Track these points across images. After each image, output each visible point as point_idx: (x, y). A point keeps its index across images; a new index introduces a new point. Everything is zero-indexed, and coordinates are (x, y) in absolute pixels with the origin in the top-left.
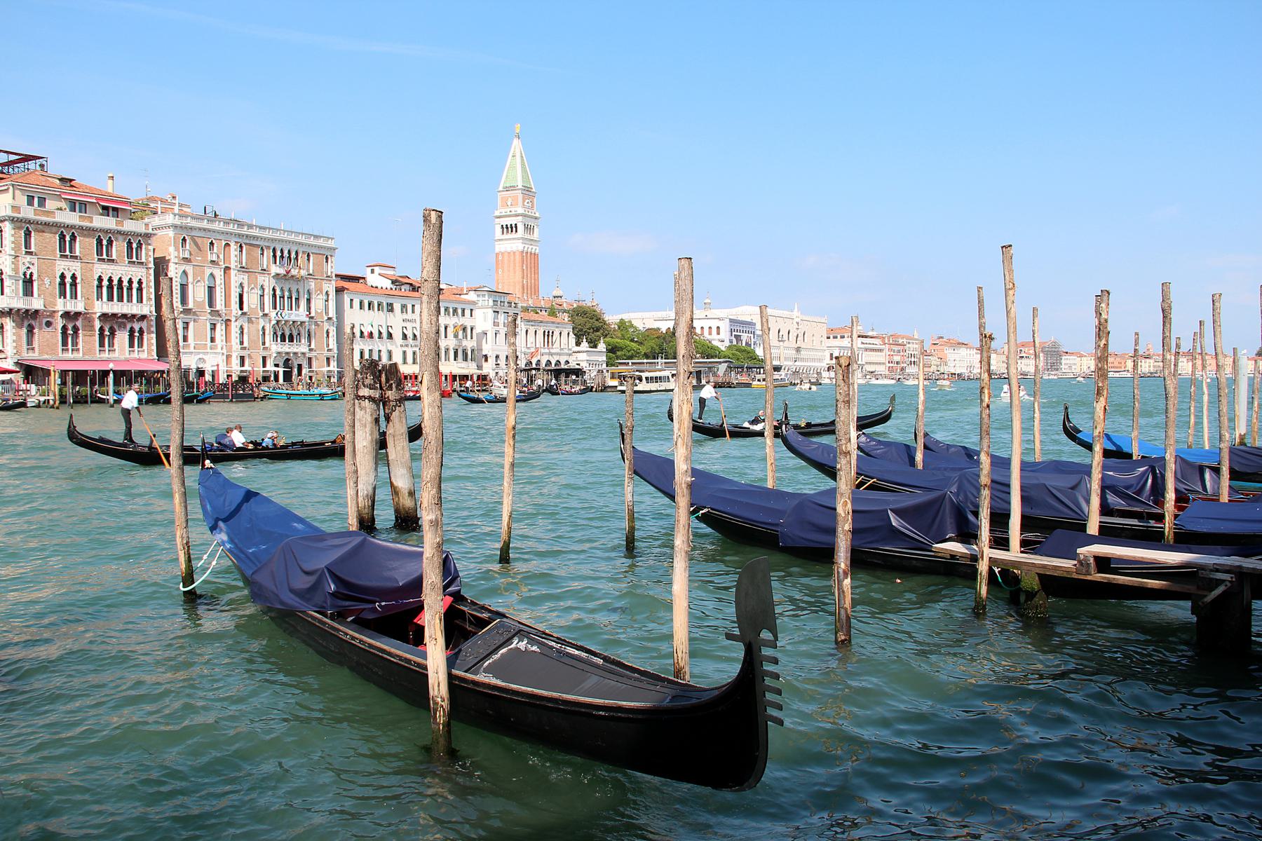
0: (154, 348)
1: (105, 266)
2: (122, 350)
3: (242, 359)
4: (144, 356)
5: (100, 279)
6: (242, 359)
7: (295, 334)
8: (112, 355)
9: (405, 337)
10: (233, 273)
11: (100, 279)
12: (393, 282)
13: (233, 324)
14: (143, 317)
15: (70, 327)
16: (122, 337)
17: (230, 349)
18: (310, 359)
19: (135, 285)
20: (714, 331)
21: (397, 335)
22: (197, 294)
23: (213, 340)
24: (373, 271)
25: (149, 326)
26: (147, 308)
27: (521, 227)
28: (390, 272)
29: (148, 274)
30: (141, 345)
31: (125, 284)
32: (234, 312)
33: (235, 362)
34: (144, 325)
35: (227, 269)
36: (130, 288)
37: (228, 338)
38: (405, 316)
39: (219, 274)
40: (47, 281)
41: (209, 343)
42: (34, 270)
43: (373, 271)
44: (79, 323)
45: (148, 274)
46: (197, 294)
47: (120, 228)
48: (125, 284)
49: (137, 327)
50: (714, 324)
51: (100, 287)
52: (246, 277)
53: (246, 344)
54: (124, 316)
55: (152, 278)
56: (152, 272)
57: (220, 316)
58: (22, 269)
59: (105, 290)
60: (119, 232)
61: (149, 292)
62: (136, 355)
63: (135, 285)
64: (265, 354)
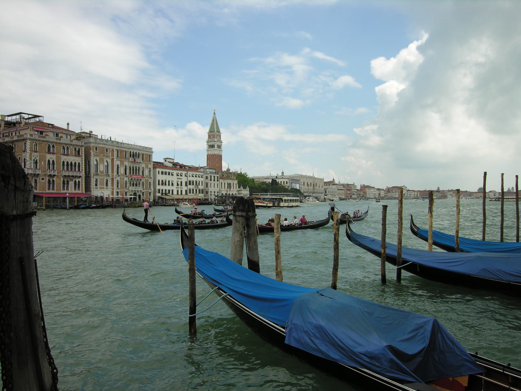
0: (84, 188)
1: (65, 157)
2: (71, 189)
3: (118, 192)
4: (80, 192)
5: (64, 162)
6: (118, 192)
7: (138, 183)
8: (67, 192)
9: (178, 185)
10: (115, 160)
11: (64, 162)
12: (173, 165)
13: (115, 179)
14: (80, 177)
15: (51, 180)
16: (71, 184)
17: (113, 189)
18: (143, 193)
19: (77, 165)
20: (285, 183)
22: (101, 168)
23: (107, 185)
24: (166, 161)
25: (82, 180)
26: (83, 174)
27: (216, 146)
28: (172, 161)
29: (82, 161)
31: (73, 164)
32: (115, 175)
33: (115, 193)
34: (80, 180)
35: (113, 160)
36: (75, 166)
37: (113, 185)
40: (43, 163)
41: (105, 187)
42: (38, 158)
43: (166, 161)
44: (55, 179)
45: (82, 161)
47: (71, 143)
48: (73, 164)
49: (77, 180)
50: (285, 180)
51: (63, 165)
53: (119, 187)
54: (73, 176)
55: (84, 162)
56: (83, 160)
58: (33, 158)
59: (65, 166)
60: (71, 145)
61: (83, 167)
62: (77, 191)
63: (77, 165)
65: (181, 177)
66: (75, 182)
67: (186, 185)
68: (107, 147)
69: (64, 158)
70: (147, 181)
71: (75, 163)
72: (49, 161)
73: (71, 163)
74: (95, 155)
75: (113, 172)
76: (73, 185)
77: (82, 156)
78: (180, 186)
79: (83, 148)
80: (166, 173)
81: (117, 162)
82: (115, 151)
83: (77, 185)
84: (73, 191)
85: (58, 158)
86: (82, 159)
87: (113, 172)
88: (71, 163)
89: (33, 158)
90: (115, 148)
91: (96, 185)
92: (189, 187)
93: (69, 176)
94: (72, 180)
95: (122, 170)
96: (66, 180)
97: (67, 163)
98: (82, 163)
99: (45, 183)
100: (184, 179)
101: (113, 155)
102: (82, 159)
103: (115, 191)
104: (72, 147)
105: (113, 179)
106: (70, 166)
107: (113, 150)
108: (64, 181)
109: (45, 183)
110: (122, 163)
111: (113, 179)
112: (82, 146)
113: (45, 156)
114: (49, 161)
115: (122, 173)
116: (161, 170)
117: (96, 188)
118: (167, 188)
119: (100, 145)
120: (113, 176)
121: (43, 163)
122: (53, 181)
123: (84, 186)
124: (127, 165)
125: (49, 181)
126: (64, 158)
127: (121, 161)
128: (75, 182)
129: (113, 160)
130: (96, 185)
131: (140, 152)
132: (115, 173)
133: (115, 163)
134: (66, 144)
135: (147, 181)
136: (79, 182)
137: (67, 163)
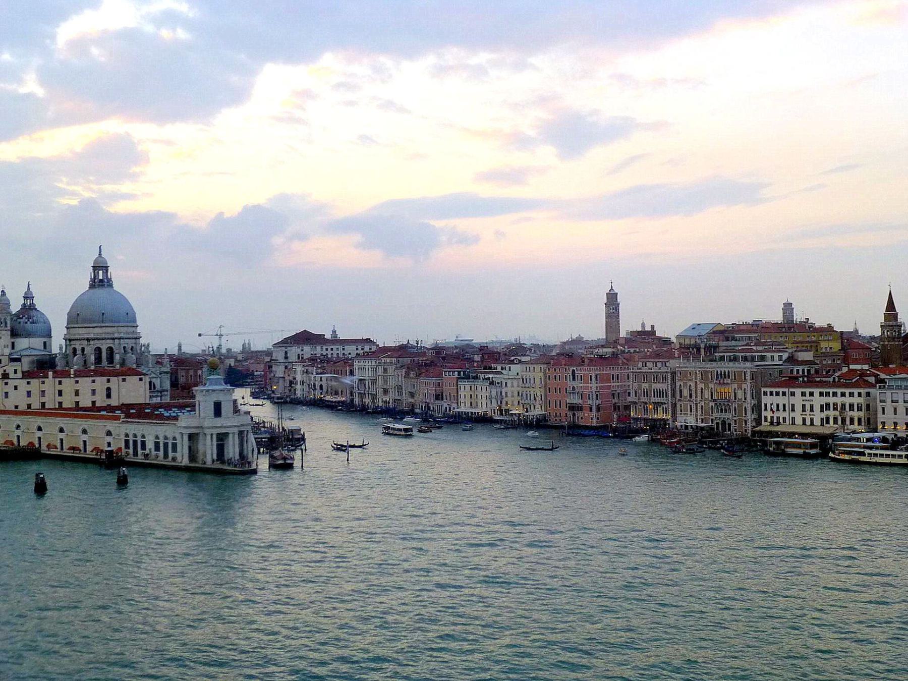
16: (660, 409)
21: (799, 408)
22: (686, 393)
38: (804, 398)
39: (693, 385)
65: (811, 398)
67: (822, 411)
78: (808, 412)
80: (777, 394)
81: (701, 386)
92: (826, 413)
95: (707, 394)
100: (818, 401)
101: (696, 378)
106: (661, 394)
110: (706, 386)
116: (768, 390)
132: (699, 398)
135: (740, 406)
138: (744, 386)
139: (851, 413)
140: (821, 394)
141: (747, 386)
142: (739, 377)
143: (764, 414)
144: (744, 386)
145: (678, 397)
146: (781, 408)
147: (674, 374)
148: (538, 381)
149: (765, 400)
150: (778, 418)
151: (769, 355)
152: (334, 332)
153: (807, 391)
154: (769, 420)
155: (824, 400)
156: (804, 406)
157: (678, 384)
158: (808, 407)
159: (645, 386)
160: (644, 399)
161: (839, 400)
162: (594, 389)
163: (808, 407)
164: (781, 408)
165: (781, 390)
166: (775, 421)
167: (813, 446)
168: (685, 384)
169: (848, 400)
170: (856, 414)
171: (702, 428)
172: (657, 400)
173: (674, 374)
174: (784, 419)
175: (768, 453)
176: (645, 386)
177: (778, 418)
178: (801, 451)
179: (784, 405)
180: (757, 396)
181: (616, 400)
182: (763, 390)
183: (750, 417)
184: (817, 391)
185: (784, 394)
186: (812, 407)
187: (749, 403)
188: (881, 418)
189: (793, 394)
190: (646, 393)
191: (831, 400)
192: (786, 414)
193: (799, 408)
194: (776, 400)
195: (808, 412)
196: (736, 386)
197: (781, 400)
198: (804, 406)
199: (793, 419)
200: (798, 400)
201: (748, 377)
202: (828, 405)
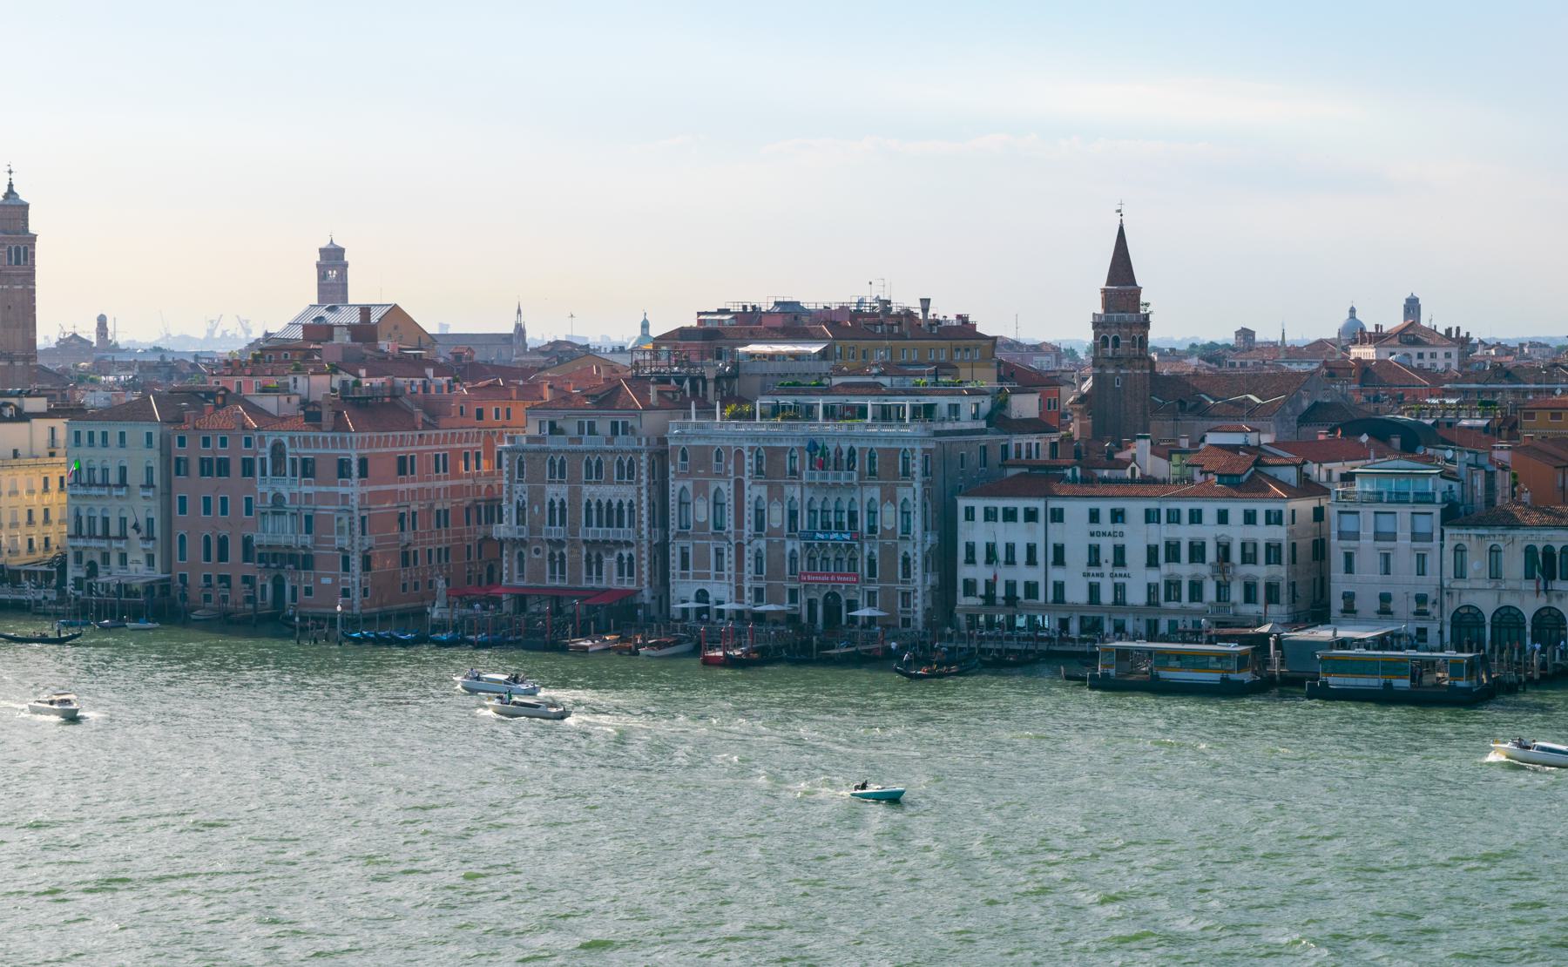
1: (593, 488)
2: (610, 579)
5: (588, 504)
11: (588, 504)
13: (747, 548)
16: (610, 561)
17: (740, 579)
21: (1077, 556)
22: (701, 511)
23: (719, 567)
30: (631, 574)
34: (634, 551)
35: (739, 485)
38: (1095, 527)
39: (727, 488)
40: (536, 509)
41: (712, 571)
44: (565, 550)
45: (639, 494)
46: (701, 511)
48: (615, 506)
49: (625, 553)
52: (764, 489)
57: (727, 539)
58: (515, 498)
64: (794, 586)
65: (1119, 527)
66: (621, 557)
67: (1152, 561)
68: (718, 443)
69: (590, 491)
70: (888, 552)
71: (620, 504)
72: (552, 503)
73: (609, 503)
74: (678, 476)
75: (739, 524)
76: (615, 567)
77: (639, 481)
78: (1107, 568)
79: (644, 457)
80: (1010, 515)
81: (754, 492)
82: (747, 454)
83: (627, 567)
84: (615, 585)
85: (575, 493)
86: (639, 489)
87: (739, 524)
88: (609, 503)
89: (515, 498)
90: (747, 445)
91: (685, 566)
92: (1166, 569)
93: (606, 542)
94: (610, 552)
95: (776, 517)
96: (594, 554)
97: (599, 503)
98: (640, 502)
99: (542, 562)
100: (1138, 537)
101: (739, 469)
102: (639, 489)
103: (747, 585)
104: (609, 458)
105: (740, 548)
106: (612, 514)
107: (739, 453)
108: (588, 556)
109: (542, 562)
110: (775, 493)
111: (740, 548)
112: (638, 452)
113: (542, 490)
114: (552, 503)
115: (776, 525)
116: (979, 504)
117: (682, 576)
118: (1022, 574)
119: (694, 443)
120: (739, 536)
121: (536, 509)
122: (562, 555)
123: (645, 569)
124: (797, 495)
125: (552, 556)
126: (590, 491)
127: (770, 486)
128: (621, 557)
129: (739, 485)
130: (685, 566)
131: (856, 446)
132: (749, 528)
133: (747, 492)
134: (594, 452)
135: (888, 552)
136: (631, 558)
137: (599, 503)
138: (903, 493)
139: (1249, 569)
140: (1151, 517)
141: (912, 492)
142: (885, 467)
143: (964, 572)
144: (903, 493)
145: (674, 526)
146: (1021, 555)
147: (660, 456)
148: (136, 477)
149: (976, 533)
150: (1011, 586)
151: (943, 402)
152: (102, 322)
153: (1105, 507)
154: (981, 590)
155: (1161, 533)
156: (1094, 551)
157: (675, 487)
158: (1107, 554)
159: (556, 492)
160: (557, 532)
161: (1209, 532)
162: (355, 502)
163: (1107, 554)
164: (1021, 555)
165: (1021, 504)
166: (1000, 591)
167: (1242, 662)
168: (701, 489)
169: (1236, 532)
170: (1261, 572)
171: (759, 618)
172: (602, 533)
173: (660, 456)
174: (1031, 589)
175: (1104, 685)
176: (556, 492)
177: (1011, 586)
178: (1213, 677)
179: (1031, 549)
180: (945, 524)
181: (408, 536)
182: (963, 503)
183: (921, 582)
184: (1135, 509)
185: (1031, 516)
186: (1119, 552)
187: (918, 545)
188: (1339, 583)
189: (1057, 516)
190: (558, 513)
191: (1185, 533)
192: (1034, 574)
193: (1077, 556)
194: (1003, 533)
195: (1107, 568)
196: (875, 493)
197: (1019, 534)
198: (1094, 551)
199: (1059, 587)
200: (1075, 532)
201: (917, 469)
202: (1173, 552)
